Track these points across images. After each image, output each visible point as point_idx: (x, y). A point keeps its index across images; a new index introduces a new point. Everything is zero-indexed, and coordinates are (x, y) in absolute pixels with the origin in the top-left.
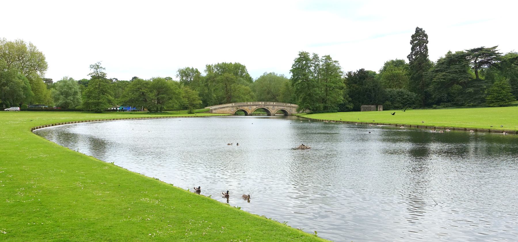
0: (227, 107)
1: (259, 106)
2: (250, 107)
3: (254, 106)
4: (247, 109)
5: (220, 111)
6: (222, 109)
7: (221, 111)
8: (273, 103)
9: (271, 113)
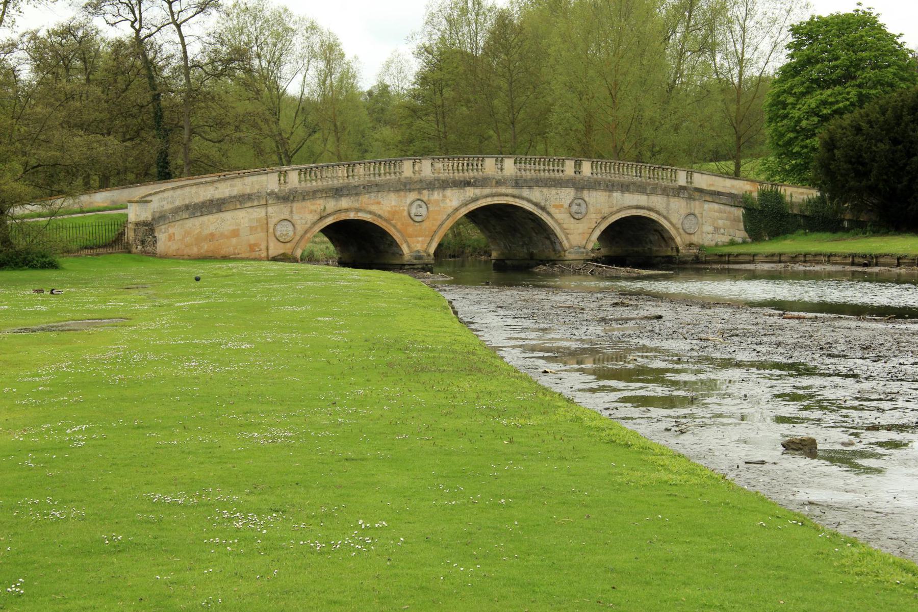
0: (243, 200)
1: (477, 191)
2: (413, 196)
3: (449, 192)
4: (394, 213)
5: (188, 240)
6: (205, 219)
7: (199, 239)
9: (566, 244)
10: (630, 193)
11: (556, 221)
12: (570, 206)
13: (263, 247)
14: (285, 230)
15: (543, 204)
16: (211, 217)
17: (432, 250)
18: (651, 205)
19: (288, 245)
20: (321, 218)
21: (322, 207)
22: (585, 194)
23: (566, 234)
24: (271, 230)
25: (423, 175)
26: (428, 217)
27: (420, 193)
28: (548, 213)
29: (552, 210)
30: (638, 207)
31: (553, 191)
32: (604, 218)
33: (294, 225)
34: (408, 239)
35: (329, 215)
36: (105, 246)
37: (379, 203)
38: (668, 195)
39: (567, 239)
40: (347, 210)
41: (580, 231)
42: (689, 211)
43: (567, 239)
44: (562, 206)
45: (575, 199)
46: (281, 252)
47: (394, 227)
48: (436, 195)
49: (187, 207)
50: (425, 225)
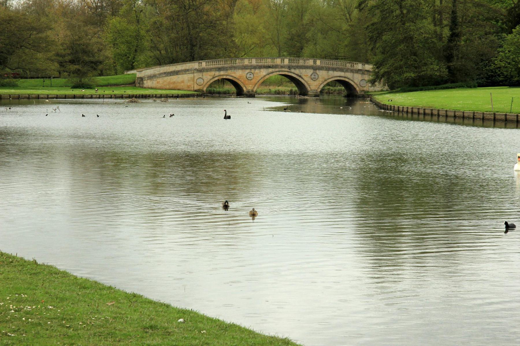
0: (186, 71)
1: (273, 70)
2: (248, 71)
3: (262, 70)
4: (240, 77)
5: (165, 83)
6: (172, 77)
7: (169, 83)
8: (315, 62)
9: (309, 89)
10: (336, 71)
11: (305, 81)
12: (311, 75)
13: (192, 86)
14: (200, 81)
15: (300, 74)
16: (174, 76)
17: (319, 90)
18: (345, 76)
19: (201, 86)
20: (213, 78)
21: (214, 74)
22: (317, 71)
23: (309, 85)
24: (195, 81)
25: (252, 64)
26: (253, 78)
27: (251, 70)
28: (302, 78)
29: (304, 77)
30: (340, 77)
31: (304, 70)
32: (325, 80)
33: (203, 80)
34: (246, 86)
35: (216, 77)
36: (130, 84)
37: (235, 73)
38: (353, 72)
39: (310, 87)
40: (223, 75)
41: (315, 84)
42: (362, 79)
43: (310, 87)
44: (308, 76)
45: (313, 73)
46: (199, 88)
47: (240, 81)
48: (257, 71)
49: (165, 73)
50: (252, 81)
